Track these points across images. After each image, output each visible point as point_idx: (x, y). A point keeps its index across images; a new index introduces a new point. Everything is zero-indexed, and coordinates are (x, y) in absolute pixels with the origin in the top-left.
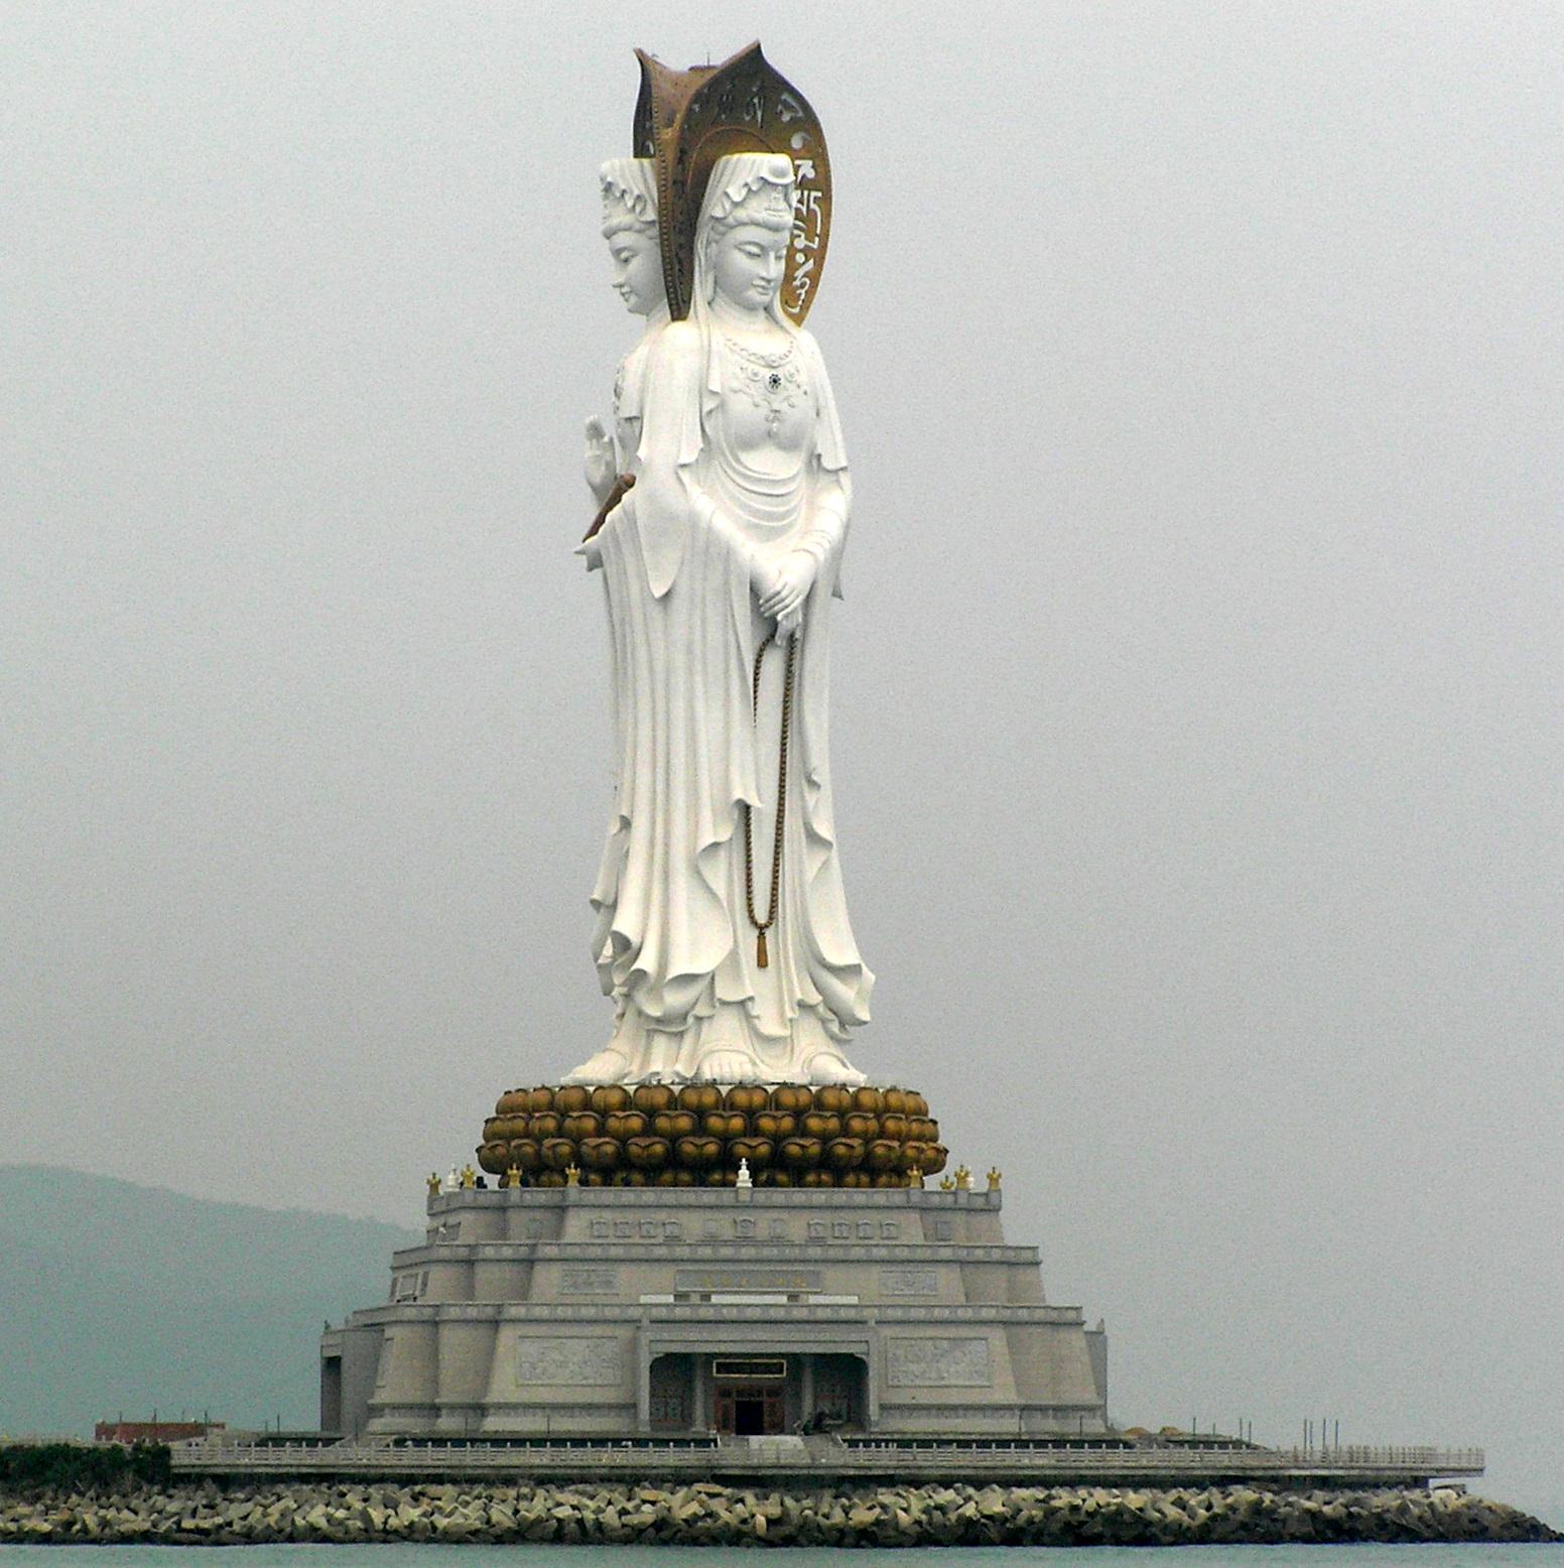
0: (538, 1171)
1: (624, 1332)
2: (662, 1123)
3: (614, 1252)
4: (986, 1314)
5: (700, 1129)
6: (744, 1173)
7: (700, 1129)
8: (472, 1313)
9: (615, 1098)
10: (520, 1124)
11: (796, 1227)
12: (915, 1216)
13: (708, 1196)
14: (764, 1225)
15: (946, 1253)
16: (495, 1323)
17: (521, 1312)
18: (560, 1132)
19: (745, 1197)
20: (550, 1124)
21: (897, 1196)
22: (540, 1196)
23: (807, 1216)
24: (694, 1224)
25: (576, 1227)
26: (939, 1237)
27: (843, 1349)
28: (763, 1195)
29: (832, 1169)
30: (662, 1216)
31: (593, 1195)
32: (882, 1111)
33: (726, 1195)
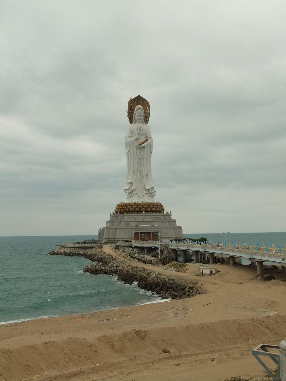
0: (121, 212)
1: (131, 229)
2: (133, 207)
3: (130, 221)
4: (171, 227)
5: (137, 207)
6: (144, 212)
7: (137, 207)
8: (114, 228)
9: (133, 204)
10: (122, 207)
11: (150, 217)
12: (163, 216)
13: (140, 214)
14: (146, 217)
15: (166, 220)
16: (116, 229)
17: (119, 228)
18: (127, 208)
19: (144, 214)
20: (126, 207)
21: (161, 214)
22: (122, 215)
23: (150, 217)
24: (138, 218)
25: (125, 218)
26: (165, 218)
27: (156, 231)
28: (146, 214)
29: (156, 212)
30: (135, 217)
31: (127, 215)
32: (157, 206)
33: (142, 214)
